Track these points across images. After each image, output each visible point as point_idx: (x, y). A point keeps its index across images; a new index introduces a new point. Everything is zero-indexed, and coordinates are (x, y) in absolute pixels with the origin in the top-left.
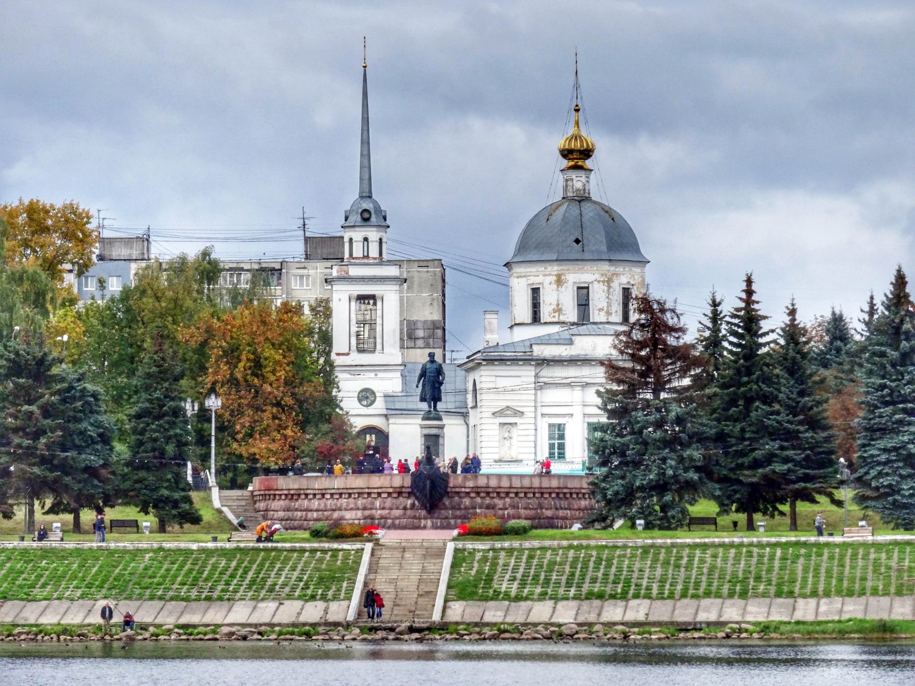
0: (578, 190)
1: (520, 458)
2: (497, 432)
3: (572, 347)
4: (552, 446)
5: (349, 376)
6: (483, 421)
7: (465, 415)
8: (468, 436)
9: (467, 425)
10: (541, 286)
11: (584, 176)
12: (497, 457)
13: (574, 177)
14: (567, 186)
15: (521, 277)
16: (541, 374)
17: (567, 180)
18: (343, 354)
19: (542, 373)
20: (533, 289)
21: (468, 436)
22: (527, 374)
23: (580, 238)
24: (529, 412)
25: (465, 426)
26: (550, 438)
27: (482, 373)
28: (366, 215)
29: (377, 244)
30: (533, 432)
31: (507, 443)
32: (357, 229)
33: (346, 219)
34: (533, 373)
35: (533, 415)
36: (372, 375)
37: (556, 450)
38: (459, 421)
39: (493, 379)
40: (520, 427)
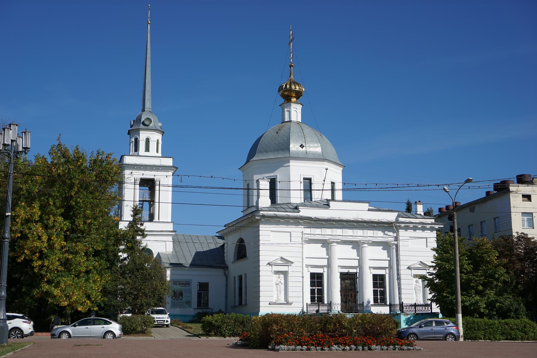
4: (312, 292)
22: (297, 231)
23: (304, 145)
25: (224, 278)
26: (312, 285)
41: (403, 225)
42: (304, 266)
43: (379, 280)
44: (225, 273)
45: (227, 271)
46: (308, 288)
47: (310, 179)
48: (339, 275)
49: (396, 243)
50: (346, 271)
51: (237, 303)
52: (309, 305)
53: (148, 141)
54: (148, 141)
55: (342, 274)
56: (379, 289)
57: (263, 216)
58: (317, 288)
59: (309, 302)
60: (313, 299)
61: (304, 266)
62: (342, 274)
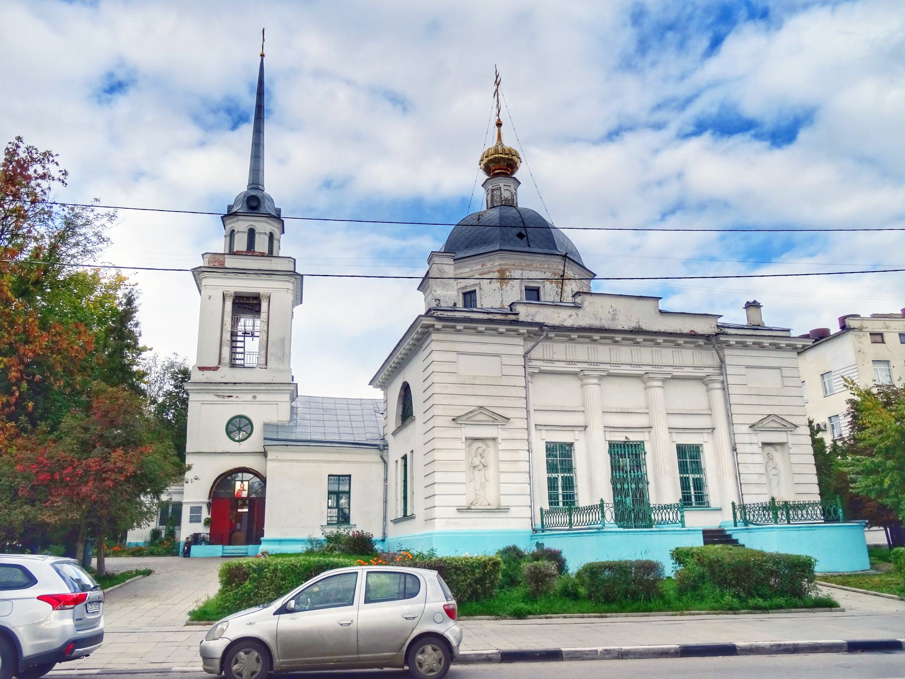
0: (506, 200)
1: (505, 501)
2: (461, 455)
3: (580, 312)
5: (216, 399)
6: (436, 433)
7: (382, 447)
8: (386, 480)
10: (477, 288)
11: (513, 186)
12: (463, 502)
13: (501, 185)
14: (492, 196)
16: (535, 354)
18: (209, 369)
19: (537, 353)
20: (464, 294)
21: (386, 480)
24: (516, 415)
25: (382, 465)
27: (434, 346)
28: (254, 204)
29: (267, 238)
30: (524, 455)
31: (478, 475)
32: (240, 218)
34: (521, 351)
35: (523, 424)
36: (249, 397)
37: (560, 491)
39: (452, 357)
40: (502, 445)
41: (732, 341)
43: (689, 458)
44: (382, 457)
45: (385, 452)
46: (542, 475)
49: (721, 378)
50: (619, 437)
51: (400, 514)
52: (548, 512)
53: (252, 233)
54: (252, 233)
55: (612, 445)
56: (691, 476)
58: (560, 475)
59: (547, 507)
60: (553, 500)
62: (612, 445)
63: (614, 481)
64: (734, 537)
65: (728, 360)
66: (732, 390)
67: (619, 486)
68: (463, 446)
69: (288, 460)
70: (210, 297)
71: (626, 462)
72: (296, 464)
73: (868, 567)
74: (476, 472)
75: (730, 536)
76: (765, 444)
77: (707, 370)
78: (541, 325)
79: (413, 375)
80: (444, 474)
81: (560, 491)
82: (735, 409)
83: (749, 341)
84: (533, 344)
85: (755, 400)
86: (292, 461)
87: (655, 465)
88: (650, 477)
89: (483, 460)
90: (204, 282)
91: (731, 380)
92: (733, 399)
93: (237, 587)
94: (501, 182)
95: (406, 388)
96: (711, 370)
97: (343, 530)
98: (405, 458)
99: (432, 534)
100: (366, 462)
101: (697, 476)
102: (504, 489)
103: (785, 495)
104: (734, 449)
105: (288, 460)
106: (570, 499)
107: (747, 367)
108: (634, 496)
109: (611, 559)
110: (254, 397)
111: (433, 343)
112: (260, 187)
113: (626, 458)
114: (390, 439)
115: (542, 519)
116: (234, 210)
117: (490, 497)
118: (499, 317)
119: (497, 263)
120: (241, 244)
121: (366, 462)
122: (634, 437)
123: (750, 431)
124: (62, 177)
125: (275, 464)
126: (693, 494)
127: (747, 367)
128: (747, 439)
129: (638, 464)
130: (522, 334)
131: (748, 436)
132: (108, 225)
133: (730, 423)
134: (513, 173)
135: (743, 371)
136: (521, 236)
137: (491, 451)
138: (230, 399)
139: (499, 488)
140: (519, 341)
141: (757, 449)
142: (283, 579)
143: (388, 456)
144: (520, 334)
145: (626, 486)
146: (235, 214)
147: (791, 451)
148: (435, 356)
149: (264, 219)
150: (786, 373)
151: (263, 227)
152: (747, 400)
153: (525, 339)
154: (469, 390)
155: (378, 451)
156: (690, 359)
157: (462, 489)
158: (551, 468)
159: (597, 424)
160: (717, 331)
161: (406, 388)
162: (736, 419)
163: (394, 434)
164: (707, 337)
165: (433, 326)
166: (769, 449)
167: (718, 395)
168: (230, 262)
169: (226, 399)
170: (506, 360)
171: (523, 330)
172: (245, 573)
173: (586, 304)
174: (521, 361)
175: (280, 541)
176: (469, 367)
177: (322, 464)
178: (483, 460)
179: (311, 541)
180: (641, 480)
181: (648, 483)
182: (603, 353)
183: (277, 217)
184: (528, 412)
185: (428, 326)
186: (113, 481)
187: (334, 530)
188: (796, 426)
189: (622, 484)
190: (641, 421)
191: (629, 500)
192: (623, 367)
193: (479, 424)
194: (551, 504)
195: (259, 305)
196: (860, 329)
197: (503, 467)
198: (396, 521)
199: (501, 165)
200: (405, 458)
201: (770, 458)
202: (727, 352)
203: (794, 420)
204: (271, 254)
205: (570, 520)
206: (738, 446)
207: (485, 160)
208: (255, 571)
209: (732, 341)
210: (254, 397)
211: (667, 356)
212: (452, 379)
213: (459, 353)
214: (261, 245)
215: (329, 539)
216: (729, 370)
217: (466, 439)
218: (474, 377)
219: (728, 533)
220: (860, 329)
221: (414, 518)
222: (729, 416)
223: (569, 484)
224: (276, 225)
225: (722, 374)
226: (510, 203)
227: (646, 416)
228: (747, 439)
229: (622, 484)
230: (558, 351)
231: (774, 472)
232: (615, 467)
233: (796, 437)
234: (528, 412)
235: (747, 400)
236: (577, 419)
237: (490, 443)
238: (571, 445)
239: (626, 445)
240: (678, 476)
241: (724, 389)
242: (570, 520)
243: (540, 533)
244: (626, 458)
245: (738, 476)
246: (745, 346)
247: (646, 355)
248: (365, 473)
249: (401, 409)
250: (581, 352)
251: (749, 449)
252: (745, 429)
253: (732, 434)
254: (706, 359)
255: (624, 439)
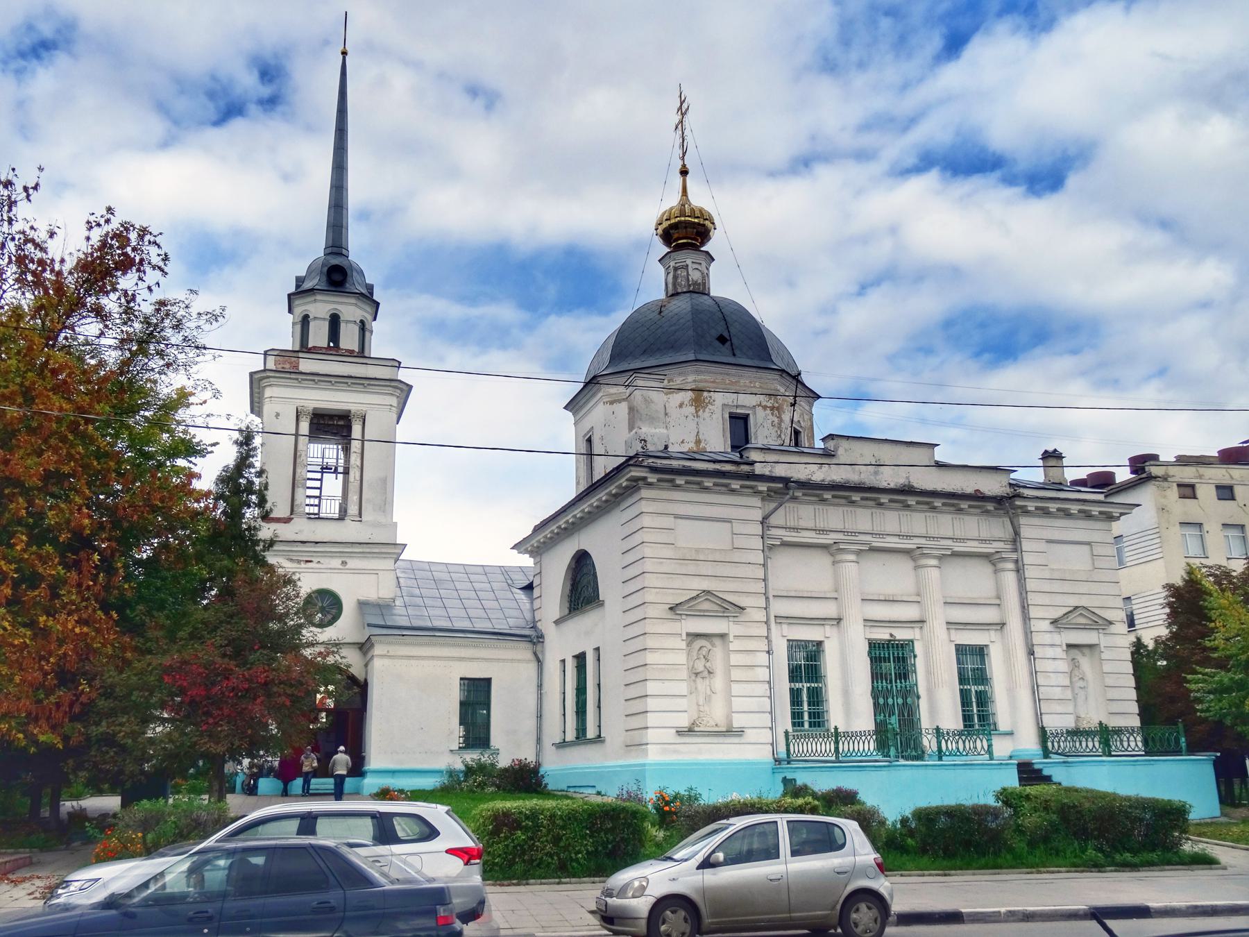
0: (695, 283)
1: (738, 721)
2: (681, 658)
4: (795, 696)
6: (649, 627)
8: (540, 686)
9: (539, 662)
11: (704, 264)
12: (684, 721)
13: (689, 262)
14: (675, 278)
15: (619, 401)
16: (776, 519)
17: (676, 269)
23: (726, 335)
25: (533, 667)
27: (644, 506)
28: (337, 277)
29: (356, 329)
30: (763, 658)
31: (701, 685)
32: (319, 297)
33: (298, 286)
34: (758, 515)
35: (761, 616)
36: (336, 563)
37: (806, 707)
38: (523, 652)
39: (668, 522)
41: (1031, 506)
42: (772, 619)
44: (535, 654)
45: (539, 647)
46: (784, 686)
47: (745, 418)
48: (865, 648)
49: (1014, 556)
50: (882, 634)
51: (571, 735)
53: (335, 321)
56: (974, 688)
57: (654, 470)
60: (797, 717)
61: (772, 619)
62: (873, 645)
63: (875, 694)
64: (1046, 772)
65: (1025, 532)
66: (1029, 572)
67: (881, 701)
68: (683, 645)
69: (402, 657)
70: (278, 415)
71: (890, 667)
72: (413, 662)
73: (1218, 813)
74: (699, 680)
75: (1040, 771)
76: (1069, 646)
77: (996, 545)
78: (786, 481)
79: (600, 541)
80: (659, 684)
81: (806, 707)
82: (1032, 598)
83: (1053, 507)
84: (773, 505)
85: (1056, 587)
86: (433, 658)
87: (929, 672)
88: (922, 690)
89: (708, 665)
90: (268, 392)
91: (1028, 559)
92: (1031, 585)
93: (506, 838)
94: (688, 258)
95: (582, 561)
96: (1001, 545)
97: (485, 758)
98: (581, 659)
99: (644, 765)
100: (512, 660)
101: (981, 688)
102: (737, 704)
103: (1093, 716)
104: (1031, 653)
105: (402, 657)
106: (818, 719)
107: (1049, 541)
108: (901, 714)
109: (946, 803)
110: (344, 563)
111: (643, 502)
112: (344, 252)
113: (891, 662)
114: (548, 628)
115: (788, 745)
116: (307, 285)
117: (716, 715)
118: (728, 467)
119: (690, 378)
120: (319, 336)
121: (512, 660)
122: (902, 634)
123: (1050, 628)
124: (161, 264)
125: (386, 662)
126: (977, 714)
127: (1049, 541)
128: (1047, 638)
129: (904, 672)
130: (761, 492)
131: (1048, 635)
132: (207, 327)
133: (1026, 618)
134: (703, 244)
135: (1042, 546)
136: (722, 339)
137: (718, 652)
138: (309, 565)
139: (730, 703)
140: (756, 501)
141: (1059, 652)
142: (563, 828)
143: (543, 652)
144: (758, 492)
145: (890, 701)
146: (311, 291)
147: (1104, 656)
148: (646, 521)
149: (353, 301)
150: (1098, 550)
151: (350, 311)
152: (1047, 586)
153: (763, 499)
154: (691, 568)
155: (529, 645)
156: (975, 530)
157: (683, 704)
158: (794, 674)
159: (855, 614)
160: (1009, 490)
161: (582, 561)
162: (1033, 612)
163: (557, 622)
164: (999, 500)
165: (645, 479)
166: (1075, 652)
167: (1010, 579)
168: (306, 365)
169: (303, 565)
170: (738, 527)
171: (763, 487)
172: (515, 821)
173: (841, 451)
174: (758, 529)
175: (393, 773)
176: (693, 536)
177: (451, 663)
178: (708, 665)
179: (451, 773)
180: (910, 693)
181: (918, 697)
182: (862, 519)
183: (368, 297)
184: (767, 598)
185: (636, 479)
186: (288, 696)
187: (472, 756)
188: (1111, 623)
189: (886, 698)
190: (910, 612)
191: (894, 720)
192: (889, 539)
193: (703, 615)
194: (794, 724)
195: (349, 428)
196: (1165, 478)
197: (736, 674)
198: (563, 744)
199: (686, 233)
200: (581, 659)
201: (1075, 664)
202: (1023, 520)
203: (1108, 615)
204: (361, 353)
205: (837, 749)
206: (1036, 649)
207: (666, 224)
208: (527, 818)
209: (1031, 506)
210: (344, 563)
211: (945, 525)
212: (667, 552)
213: (677, 517)
214: (349, 339)
215: (469, 771)
216: (1026, 545)
217: (688, 634)
218: (697, 550)
219: (1036, 767)
220: (1165, 478)
221: (603, 742)
222: (1024, 608)
223: (817, 698)
224: (369, 309)
225: (1015, 550)
226: (700, 289)
227: (916, 605)
228: (1047, 638)
229: (886, 698)
230: (804, 516)
231: (1081, 684)
232: (876, 676)
233: (1109, 638)
234: (767, 598)
235: (1047, 586)
236: (829, 609)
237: (717, 642)
238: (820, 643)
239: (891, 644)
240: (957, 687)
241: (1019, 570)
242: (837, 749)
243: (784, 765)
244: (891, 662)
245: (1035, 688)
246: (1045, 513)
247: (918, 523)
248: (510, 676)
249: (569, 587)
250: (835, 517)
251: (1050, 652)
252: (1045, 625)
253: (1028, 633)
254: (992, 530)
255: (887, 637)
